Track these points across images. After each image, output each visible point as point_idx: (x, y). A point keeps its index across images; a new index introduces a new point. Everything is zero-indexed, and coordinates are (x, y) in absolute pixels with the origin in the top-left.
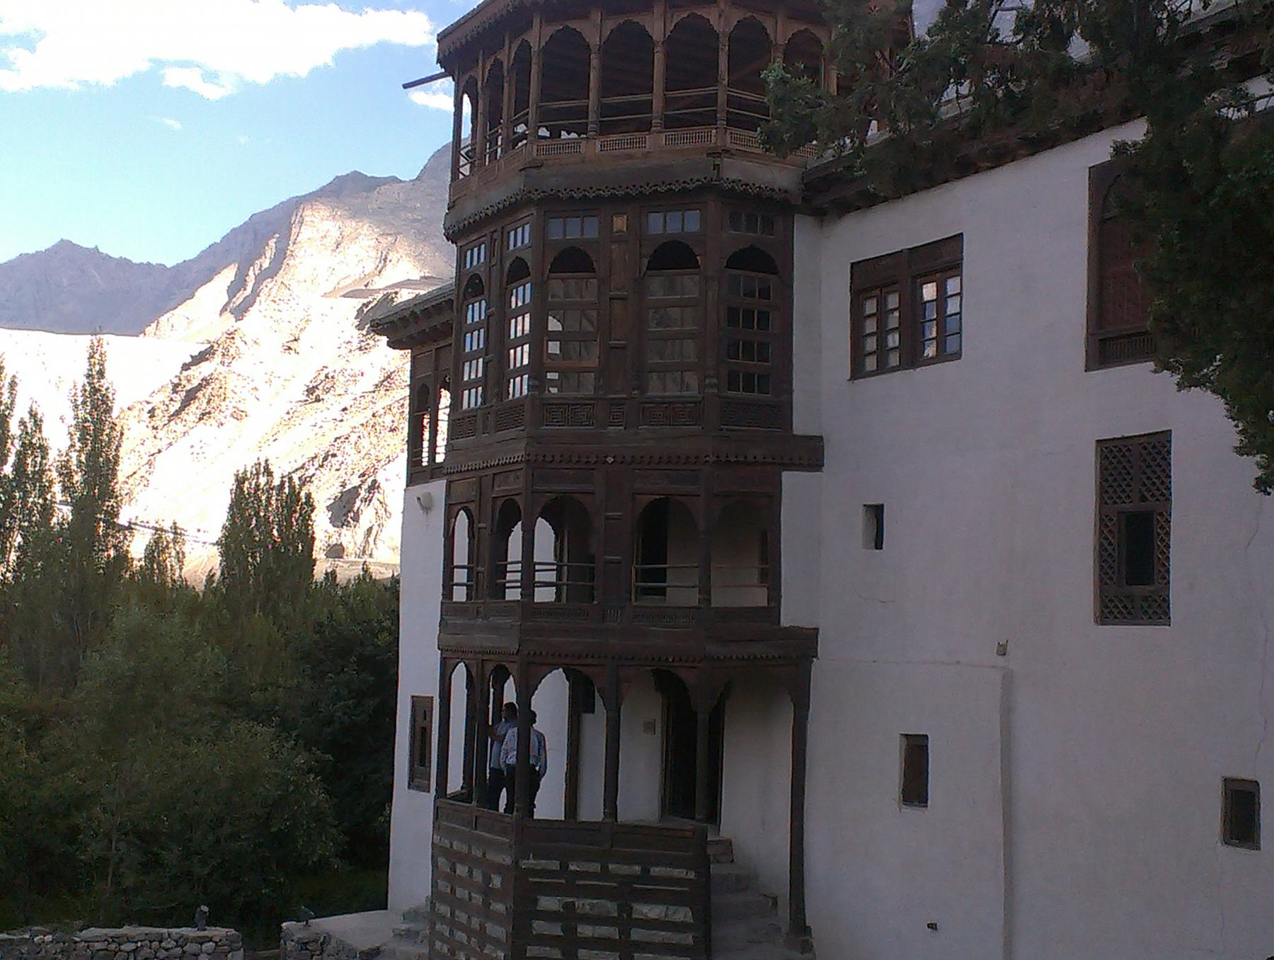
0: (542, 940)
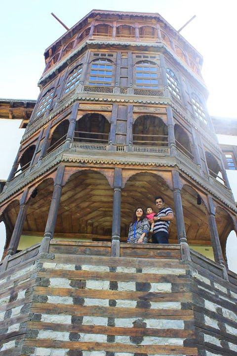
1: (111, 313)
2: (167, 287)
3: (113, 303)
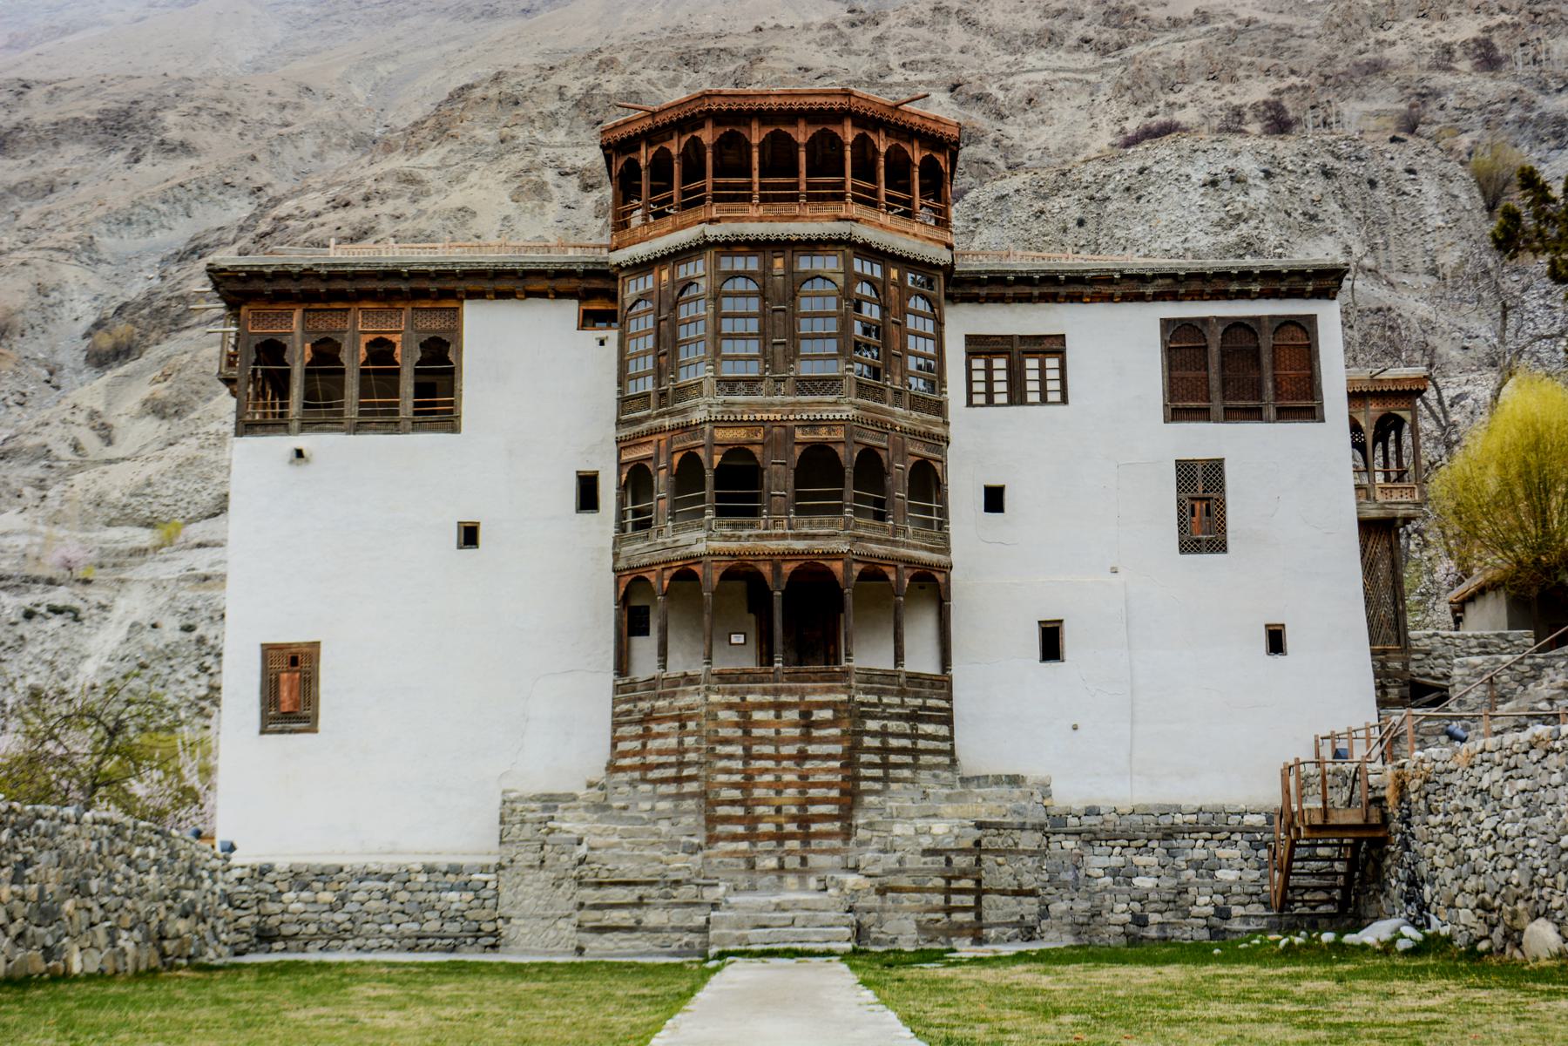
0: (869, 750)
1: (778, 741)
2: (827, 714)
3: (778, 732)
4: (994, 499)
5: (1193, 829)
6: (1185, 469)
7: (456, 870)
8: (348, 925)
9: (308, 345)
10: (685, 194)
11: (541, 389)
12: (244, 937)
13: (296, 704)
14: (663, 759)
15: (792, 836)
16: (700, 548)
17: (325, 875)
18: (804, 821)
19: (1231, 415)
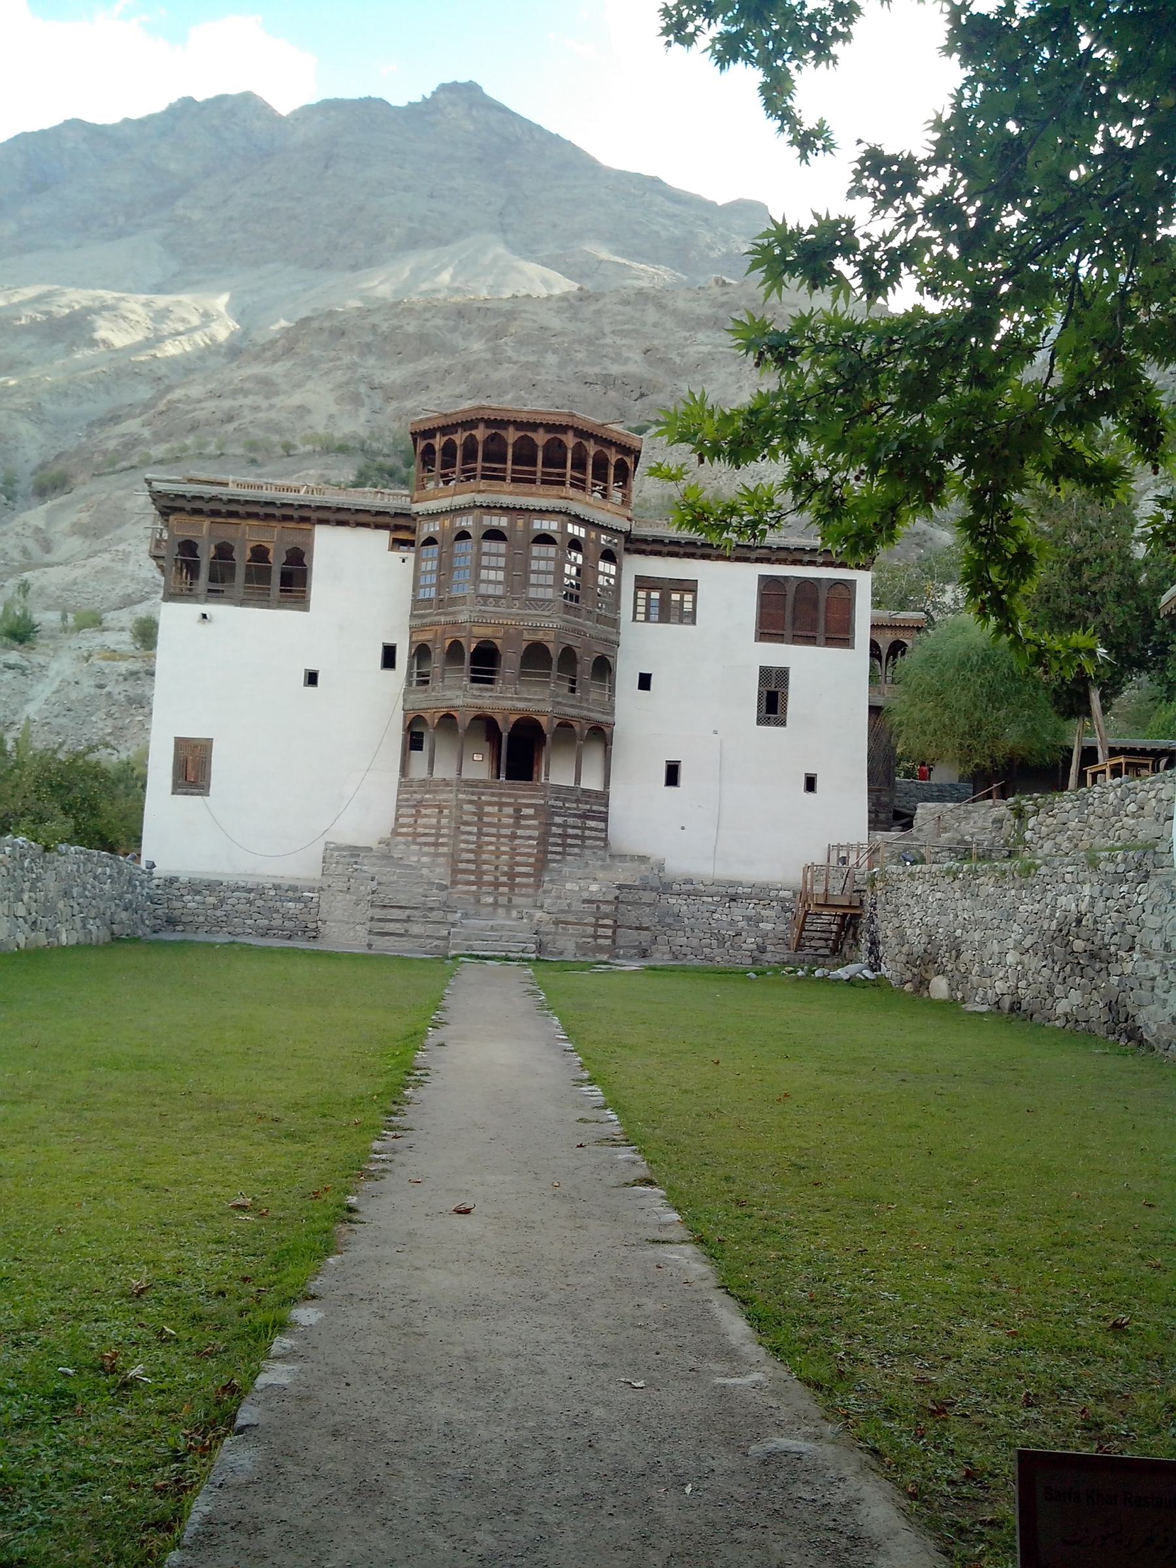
0: (555, 835)
1: (499, 826)
2: (531, 811)
3: (499, 820)
4: (645, 682)
5: (749, 897)
6: (766, 674)
7: (294, 889)
8: (224, 919)
9: (213, 546)
10: (464, 471)
11: (361, 584)
12: (159, 921)
13: (196, 777)
14: (427, 831)
15: (504, 884)
16: (459, 702)
17: (212, 886)
18: (512, 876)
19: (797, 639)
